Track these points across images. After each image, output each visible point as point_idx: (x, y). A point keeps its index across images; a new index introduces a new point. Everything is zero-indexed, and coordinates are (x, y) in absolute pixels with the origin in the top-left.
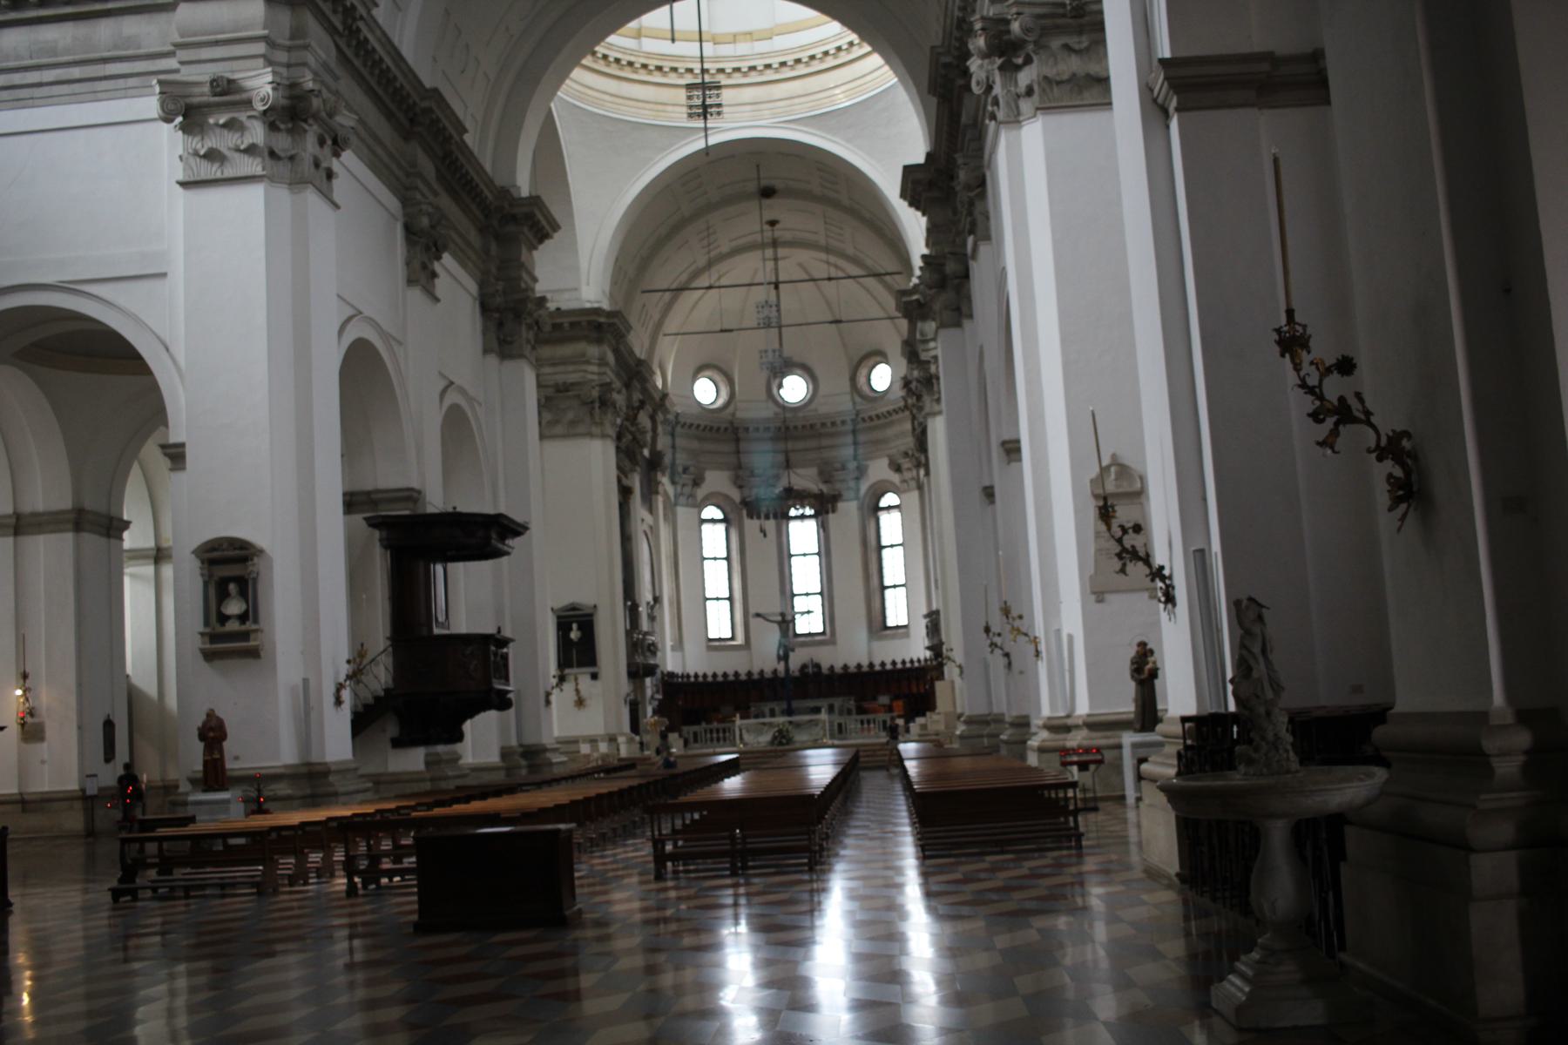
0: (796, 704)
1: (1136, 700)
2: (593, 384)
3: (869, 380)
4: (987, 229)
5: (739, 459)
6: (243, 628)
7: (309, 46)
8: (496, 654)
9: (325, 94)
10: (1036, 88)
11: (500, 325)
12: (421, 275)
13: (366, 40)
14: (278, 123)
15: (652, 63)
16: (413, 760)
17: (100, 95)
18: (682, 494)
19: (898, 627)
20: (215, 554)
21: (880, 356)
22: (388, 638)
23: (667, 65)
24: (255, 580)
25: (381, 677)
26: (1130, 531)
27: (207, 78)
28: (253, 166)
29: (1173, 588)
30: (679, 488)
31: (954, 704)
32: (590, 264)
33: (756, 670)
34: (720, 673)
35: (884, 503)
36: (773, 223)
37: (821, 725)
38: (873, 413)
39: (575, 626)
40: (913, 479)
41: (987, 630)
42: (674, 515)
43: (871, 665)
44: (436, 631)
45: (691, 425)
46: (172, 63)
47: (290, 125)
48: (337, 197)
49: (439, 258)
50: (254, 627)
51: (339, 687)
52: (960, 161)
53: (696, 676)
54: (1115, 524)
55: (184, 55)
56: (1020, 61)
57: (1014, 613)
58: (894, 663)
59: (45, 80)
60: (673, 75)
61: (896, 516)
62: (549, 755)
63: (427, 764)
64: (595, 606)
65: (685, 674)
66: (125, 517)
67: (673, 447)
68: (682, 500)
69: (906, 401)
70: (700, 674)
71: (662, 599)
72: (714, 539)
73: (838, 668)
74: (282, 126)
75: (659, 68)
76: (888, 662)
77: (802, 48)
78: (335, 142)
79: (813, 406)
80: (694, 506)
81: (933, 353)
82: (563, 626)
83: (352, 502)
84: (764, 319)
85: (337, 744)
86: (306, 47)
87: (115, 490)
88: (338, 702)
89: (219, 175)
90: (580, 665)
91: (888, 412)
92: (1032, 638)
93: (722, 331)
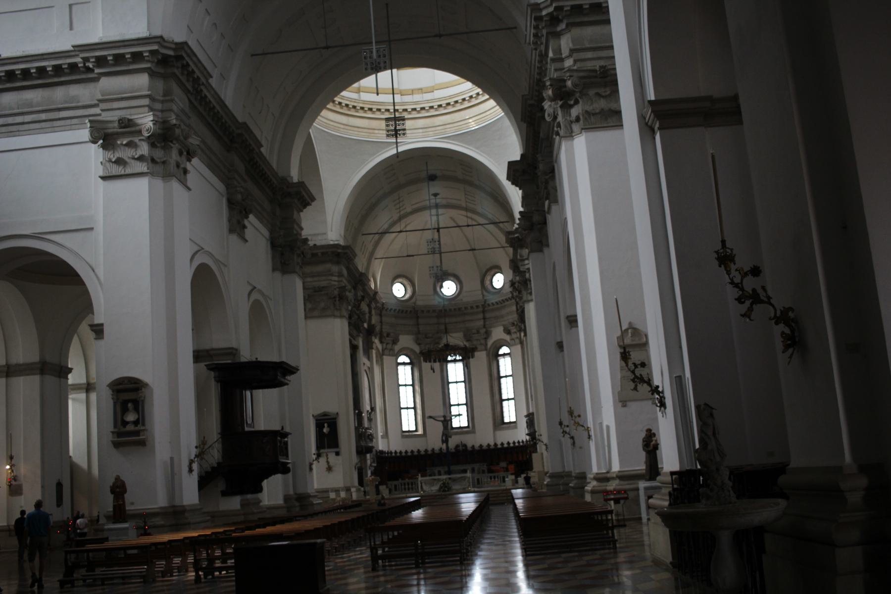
0: (453, 468)
1: (646, 463)
2: (335, 287)
4: (556, 196)
5: (418, 328)
6: (137, 428)
7: (174, 100)
8: (280, 442)
9: (183, 126)
10: (581, 117)
11: (282, 254)
12: (237, 227)
13: (206, 96)
14: (156, 143)
15: (367, 106)
16: (234, 503)
17: (56, 129)
18: (386, 349)
19: (510, 423)
20: (121, 387)
21: (497, 269)
22: (219, 434)
23: (375, 107)
24: (143, 401)
25: (215, 455)
26: (639, 366)
27: (116, 119)
28: (142, 167)
29: (664, 398)
30: (385, 345)
31: (543, 466)
32: (333, 219)
33: (430, 449)
34: (409, 451)
35: (501, 352)
36: (435, 195)
37: (467, 480)
39: (326, 425)
40: (517, 338)
41: (561, 424)
42: (382, 360)
43: (496, 445)
44: (247, 429)
46: (97, 111)
47: (163, 144)
48: (189, 184)
49: (247, 217)
50: (142, 428)
51: (191, 462)
52: (540, 159)
53: (396, 452)
54: (630, 364)
55: (104, 106)
56: (572, 102)
57: (576, 414)
58: (508, 443)
59: (26, 120)
60: (378, 113)
61: (508, 360)
62: (311, 499)
63: (242, 505)
64: (337, 414)
65: (389, 452)
66: (70, 366)
67: (381, 322)
68: (386, 352)
69: (513, 294)
70: (398, 451)
71: (376, 408)
72: (405, 374)
73: (477, 446)
74: (159, 145)
75: (370, 109)
76: (505, 442)
77: (450, 97)
78: (188, 153)
79: (461, 297)
80: (393, 355)
81: (527, 267)
82: (319, 425)
83: (198, 356)
84: (431, 249)
85: (190, 494)
86: (172, 101)
87: (64, 352)
88: (191, 470)
89: (123, 173)
90: (329, 447)
91: (503, 300)
92: (586, 428)
93: (408, 256)
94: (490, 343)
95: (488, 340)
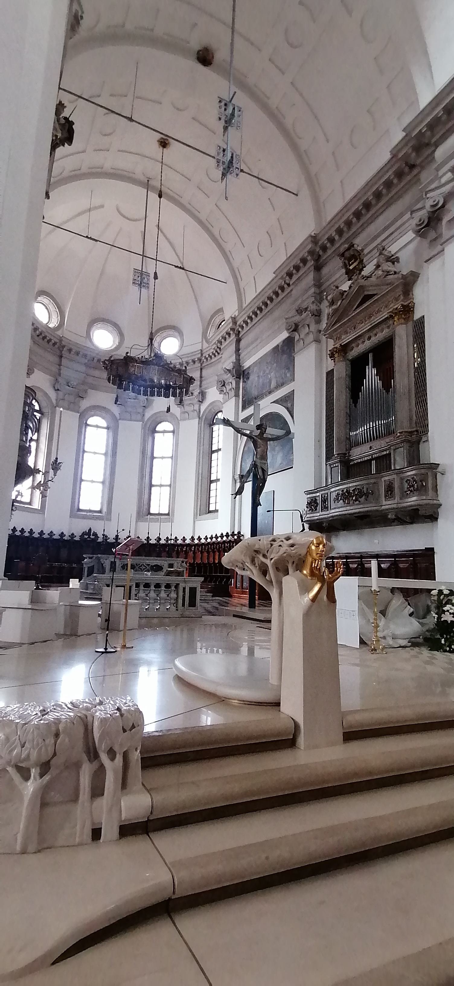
5: (60, 370)
19: (159, 514)
33: (46, 531)
35: (159, 428)
93: (87, 237)
94: (148, 414)
95: (147, 410)
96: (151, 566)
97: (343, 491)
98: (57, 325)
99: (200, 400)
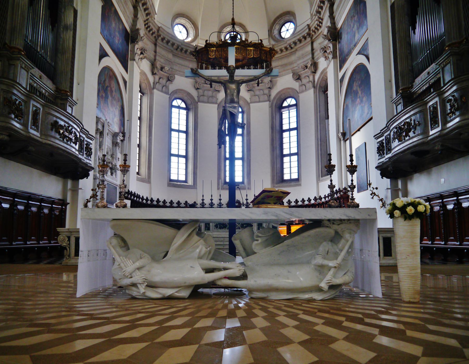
3: (280, 33)
19: (291, 180)
35: (285, 104)
38: (283, 47)
42: (152, 94)
45: (168, 42)
61: (293, 112)
65: (149, 199)
80: (167, 93)
94: (274, 93)
95: (272, 91)
96: (242, 224)
97: (396, 128)
98: (193, 38)
99: (314, 71)
